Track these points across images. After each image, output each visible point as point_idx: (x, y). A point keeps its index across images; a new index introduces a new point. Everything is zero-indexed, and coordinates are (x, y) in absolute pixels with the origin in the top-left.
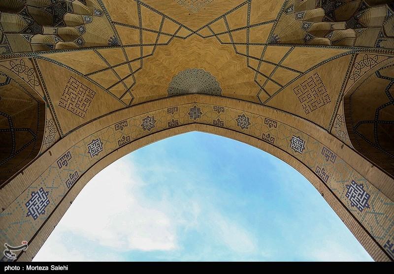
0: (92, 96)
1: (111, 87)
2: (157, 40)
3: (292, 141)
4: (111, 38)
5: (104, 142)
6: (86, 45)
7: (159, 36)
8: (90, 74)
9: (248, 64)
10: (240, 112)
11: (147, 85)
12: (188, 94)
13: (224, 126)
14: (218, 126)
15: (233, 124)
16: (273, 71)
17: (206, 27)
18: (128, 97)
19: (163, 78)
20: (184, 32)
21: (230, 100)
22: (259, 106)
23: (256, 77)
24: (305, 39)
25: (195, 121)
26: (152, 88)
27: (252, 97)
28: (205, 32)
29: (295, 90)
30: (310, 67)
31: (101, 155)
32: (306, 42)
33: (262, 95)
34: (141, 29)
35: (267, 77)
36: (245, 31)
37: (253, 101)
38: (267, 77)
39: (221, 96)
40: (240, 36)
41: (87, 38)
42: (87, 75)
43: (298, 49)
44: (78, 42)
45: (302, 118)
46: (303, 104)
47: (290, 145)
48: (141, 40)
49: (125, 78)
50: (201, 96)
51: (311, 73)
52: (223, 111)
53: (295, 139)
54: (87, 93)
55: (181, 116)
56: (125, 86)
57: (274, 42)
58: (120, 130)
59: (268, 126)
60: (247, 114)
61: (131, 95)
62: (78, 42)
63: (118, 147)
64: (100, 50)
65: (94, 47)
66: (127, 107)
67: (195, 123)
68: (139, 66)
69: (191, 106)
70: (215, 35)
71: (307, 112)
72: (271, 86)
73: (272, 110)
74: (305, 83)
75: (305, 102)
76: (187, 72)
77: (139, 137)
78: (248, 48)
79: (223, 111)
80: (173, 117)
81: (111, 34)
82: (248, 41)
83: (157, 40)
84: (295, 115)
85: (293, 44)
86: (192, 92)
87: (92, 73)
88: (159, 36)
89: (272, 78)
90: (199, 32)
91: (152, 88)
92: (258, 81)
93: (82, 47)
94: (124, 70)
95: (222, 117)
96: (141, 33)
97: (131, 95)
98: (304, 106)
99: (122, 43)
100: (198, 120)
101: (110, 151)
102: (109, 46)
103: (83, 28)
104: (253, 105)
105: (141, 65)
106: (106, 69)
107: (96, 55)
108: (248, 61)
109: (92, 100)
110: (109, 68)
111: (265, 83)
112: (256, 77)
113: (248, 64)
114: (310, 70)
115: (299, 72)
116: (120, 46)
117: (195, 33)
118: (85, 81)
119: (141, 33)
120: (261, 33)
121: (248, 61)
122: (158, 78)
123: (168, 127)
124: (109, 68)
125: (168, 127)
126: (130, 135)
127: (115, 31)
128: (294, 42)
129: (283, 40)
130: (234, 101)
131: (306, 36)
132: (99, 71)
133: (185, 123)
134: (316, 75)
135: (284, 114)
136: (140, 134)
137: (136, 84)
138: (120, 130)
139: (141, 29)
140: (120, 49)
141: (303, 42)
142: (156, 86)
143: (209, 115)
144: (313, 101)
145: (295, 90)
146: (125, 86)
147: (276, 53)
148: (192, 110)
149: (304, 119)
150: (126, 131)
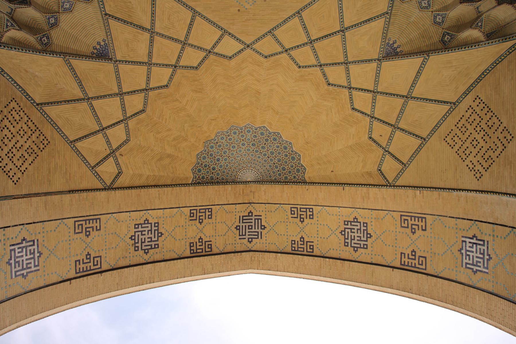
0: (42, 146)
1: (80, 139)
2: (179, 57)
3: (462, 251)
4: (99, 43)
5: (46, 253)
6: (53, 48)
7: (183, 49)
8: (48, 103)
9: (352, 103)
10: (348, 214)
11: (152, 150)
12: (235, 182)
13: (316, 252)
14: (302, 256)
15: (334, 244)
16: (402, 111)
17: (269, 37)
18: (108, 169)
19: (186, 140)
20: (228, 46)
21: (324, 187)
22: (384, 190)
23: (371, 131)
24: (443, 41)
25: (246, 247)
26: (160, 159)
27: (370, 174)
28: (267, 45)
29: (448, 139)
30: (463, 89)
31: (34, 281)
32: (447, 44)
33: (390, 167)
34: (152, 32)
35: (392, 125)
36: (337, 38)
37: (372, 183)
38: (392, 125)
39: (305, 182)
40: (329, 50)
41: (58, 37)
42: (41, 104)
43: (436, 60)
44: (41, 40)
45: (471, 191)
46: (467, 162)
47: (460, 260)
48: (150, 54)
49: (111, 126)
50: (264, 187)
51: (468, 100)
52: (311, 217)
53: (481, 265)
54: (34, 137)
55: (219, 231)
56: (108, 142)
57: (392, 53)
58: (83, 235)
59: (408, 231)
60: (363, 216)
61: (117, 164)
62: (41, 40)
63: (72, 274)
64: (75, 62)
65: (66, 54)
66: (105, 189)
67: (250, 251)
68: (140, 107)
69: (242, 210)
70: (286, 51)
71: (478, 175)
72: (403, 145)
73: (410, 191)
74: (463, 121)
75: (471, 158)
76: (235, 133)
77: (122, 264)
78: (347, 70)
79: (311, 217)
80: (201, 231)
81: (100, 36)
82: (347, 57)
83: (179, 57)
84: (457, 190)
85: (424, 52)
86: (244, 179)
87: (51, 103)
88: (183, 49)
89: (401, 125)
90: (256, 46)
91: (160, 159)
92: (375, 138)
93: (46, 48)
94: (110, 110)
95: (311, 230)
96: (152, 41)
97: (117, 164)
98: (471, 166)
99: (115, 55)
100: (257, 244)
101: (55, 279)
102: (92, 58)
103: (48, 38)
104: (373, 191)
105: (145, 104)
106: (78, 100)
107: (66, 69)
108: (351, 99)
109: (39, 153)
110: (84, 99)
111: (390, 139)
112: (371, 131)
113: (352, 103)
114: (466, 93)
115: (447, 102)
116: (111, 59)
117: (248, 46)
118: (36, 116)
119: (152, 41)
120: (366, 41)
121: (351, 99)
122: (174, 139)
123: (188, 253)
124: (84, 99)
125: (188, 253)
126: (102, 254)
127: (108, 31)
128: (425, 49)
129: (406, 49)
130: (333, 188)
131: (444, 36)
132: (65, 101)
133: (229, 249)
134: (478, 101)
135: (436, 193)
136: (125, 257)
137: (131, 144)
138: (83, 235)
139: (152, 32)
140: (109, 66)
141: (440, 46)
142: (169, 156)
143: (281, 229)
144: (483, 150)
145: (448, 139)
146: (108, 142)
147: (399, 73)
148: (243, 219)
149: (476, 191)
150: (96, 243)
